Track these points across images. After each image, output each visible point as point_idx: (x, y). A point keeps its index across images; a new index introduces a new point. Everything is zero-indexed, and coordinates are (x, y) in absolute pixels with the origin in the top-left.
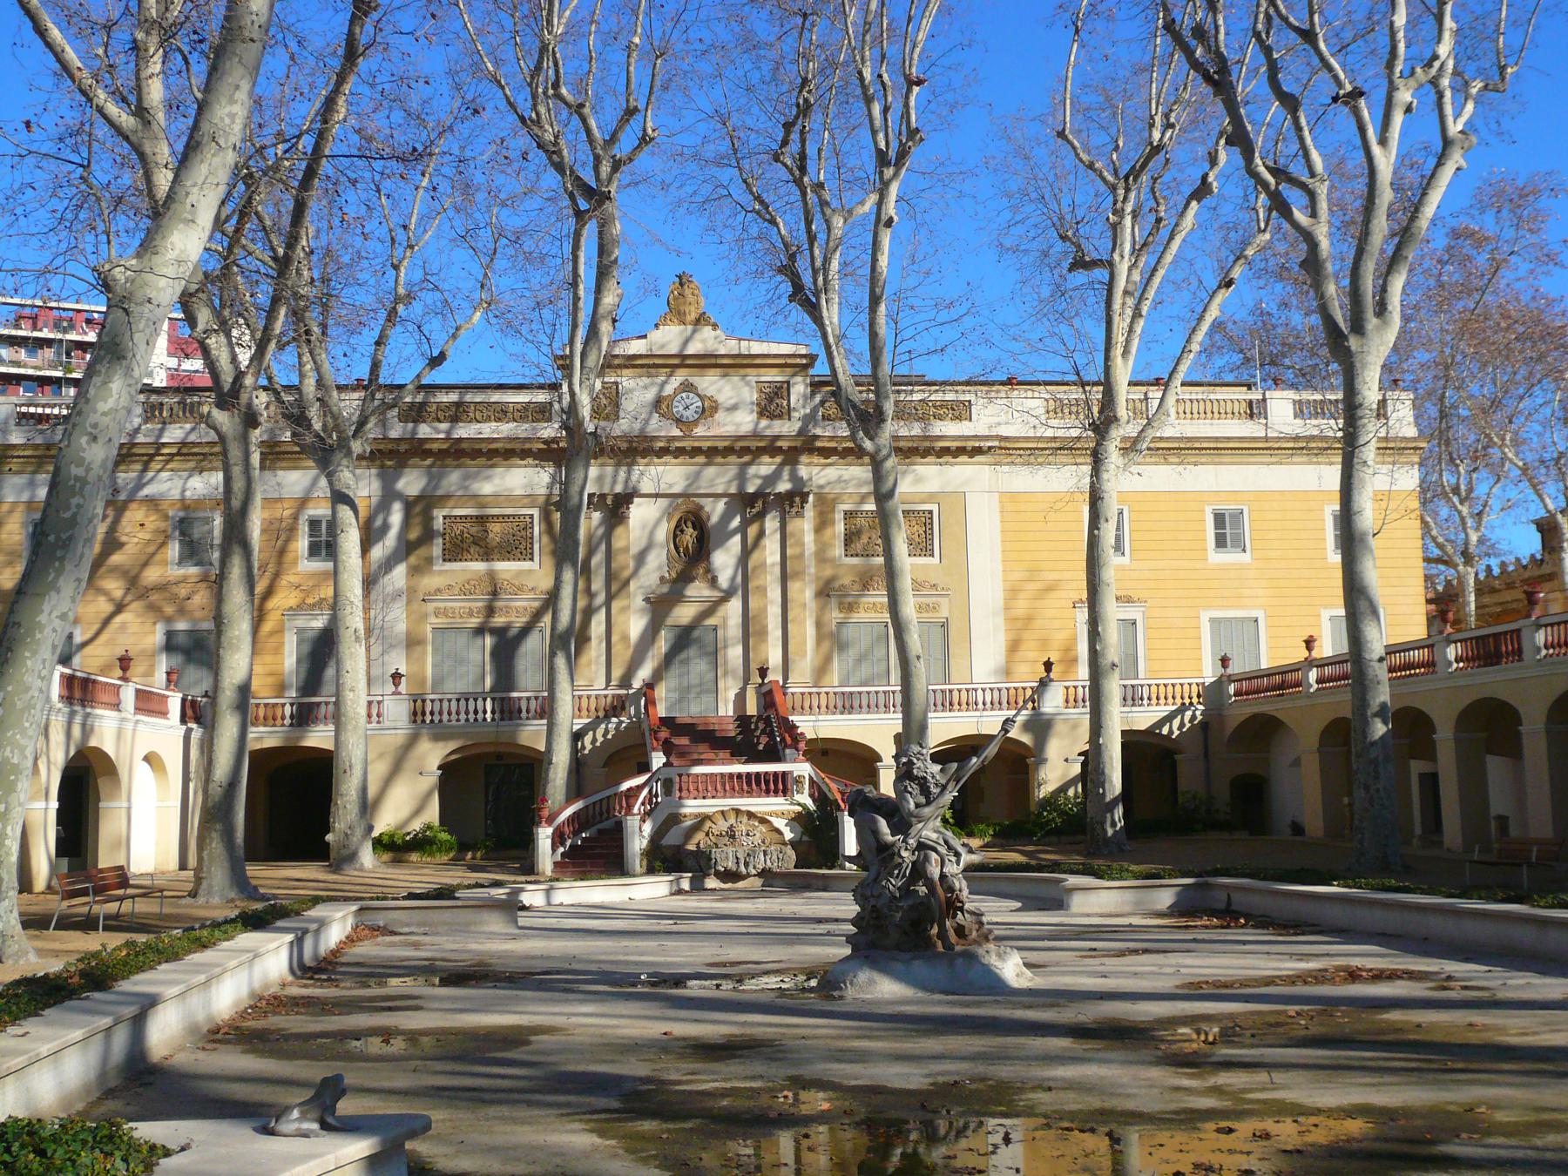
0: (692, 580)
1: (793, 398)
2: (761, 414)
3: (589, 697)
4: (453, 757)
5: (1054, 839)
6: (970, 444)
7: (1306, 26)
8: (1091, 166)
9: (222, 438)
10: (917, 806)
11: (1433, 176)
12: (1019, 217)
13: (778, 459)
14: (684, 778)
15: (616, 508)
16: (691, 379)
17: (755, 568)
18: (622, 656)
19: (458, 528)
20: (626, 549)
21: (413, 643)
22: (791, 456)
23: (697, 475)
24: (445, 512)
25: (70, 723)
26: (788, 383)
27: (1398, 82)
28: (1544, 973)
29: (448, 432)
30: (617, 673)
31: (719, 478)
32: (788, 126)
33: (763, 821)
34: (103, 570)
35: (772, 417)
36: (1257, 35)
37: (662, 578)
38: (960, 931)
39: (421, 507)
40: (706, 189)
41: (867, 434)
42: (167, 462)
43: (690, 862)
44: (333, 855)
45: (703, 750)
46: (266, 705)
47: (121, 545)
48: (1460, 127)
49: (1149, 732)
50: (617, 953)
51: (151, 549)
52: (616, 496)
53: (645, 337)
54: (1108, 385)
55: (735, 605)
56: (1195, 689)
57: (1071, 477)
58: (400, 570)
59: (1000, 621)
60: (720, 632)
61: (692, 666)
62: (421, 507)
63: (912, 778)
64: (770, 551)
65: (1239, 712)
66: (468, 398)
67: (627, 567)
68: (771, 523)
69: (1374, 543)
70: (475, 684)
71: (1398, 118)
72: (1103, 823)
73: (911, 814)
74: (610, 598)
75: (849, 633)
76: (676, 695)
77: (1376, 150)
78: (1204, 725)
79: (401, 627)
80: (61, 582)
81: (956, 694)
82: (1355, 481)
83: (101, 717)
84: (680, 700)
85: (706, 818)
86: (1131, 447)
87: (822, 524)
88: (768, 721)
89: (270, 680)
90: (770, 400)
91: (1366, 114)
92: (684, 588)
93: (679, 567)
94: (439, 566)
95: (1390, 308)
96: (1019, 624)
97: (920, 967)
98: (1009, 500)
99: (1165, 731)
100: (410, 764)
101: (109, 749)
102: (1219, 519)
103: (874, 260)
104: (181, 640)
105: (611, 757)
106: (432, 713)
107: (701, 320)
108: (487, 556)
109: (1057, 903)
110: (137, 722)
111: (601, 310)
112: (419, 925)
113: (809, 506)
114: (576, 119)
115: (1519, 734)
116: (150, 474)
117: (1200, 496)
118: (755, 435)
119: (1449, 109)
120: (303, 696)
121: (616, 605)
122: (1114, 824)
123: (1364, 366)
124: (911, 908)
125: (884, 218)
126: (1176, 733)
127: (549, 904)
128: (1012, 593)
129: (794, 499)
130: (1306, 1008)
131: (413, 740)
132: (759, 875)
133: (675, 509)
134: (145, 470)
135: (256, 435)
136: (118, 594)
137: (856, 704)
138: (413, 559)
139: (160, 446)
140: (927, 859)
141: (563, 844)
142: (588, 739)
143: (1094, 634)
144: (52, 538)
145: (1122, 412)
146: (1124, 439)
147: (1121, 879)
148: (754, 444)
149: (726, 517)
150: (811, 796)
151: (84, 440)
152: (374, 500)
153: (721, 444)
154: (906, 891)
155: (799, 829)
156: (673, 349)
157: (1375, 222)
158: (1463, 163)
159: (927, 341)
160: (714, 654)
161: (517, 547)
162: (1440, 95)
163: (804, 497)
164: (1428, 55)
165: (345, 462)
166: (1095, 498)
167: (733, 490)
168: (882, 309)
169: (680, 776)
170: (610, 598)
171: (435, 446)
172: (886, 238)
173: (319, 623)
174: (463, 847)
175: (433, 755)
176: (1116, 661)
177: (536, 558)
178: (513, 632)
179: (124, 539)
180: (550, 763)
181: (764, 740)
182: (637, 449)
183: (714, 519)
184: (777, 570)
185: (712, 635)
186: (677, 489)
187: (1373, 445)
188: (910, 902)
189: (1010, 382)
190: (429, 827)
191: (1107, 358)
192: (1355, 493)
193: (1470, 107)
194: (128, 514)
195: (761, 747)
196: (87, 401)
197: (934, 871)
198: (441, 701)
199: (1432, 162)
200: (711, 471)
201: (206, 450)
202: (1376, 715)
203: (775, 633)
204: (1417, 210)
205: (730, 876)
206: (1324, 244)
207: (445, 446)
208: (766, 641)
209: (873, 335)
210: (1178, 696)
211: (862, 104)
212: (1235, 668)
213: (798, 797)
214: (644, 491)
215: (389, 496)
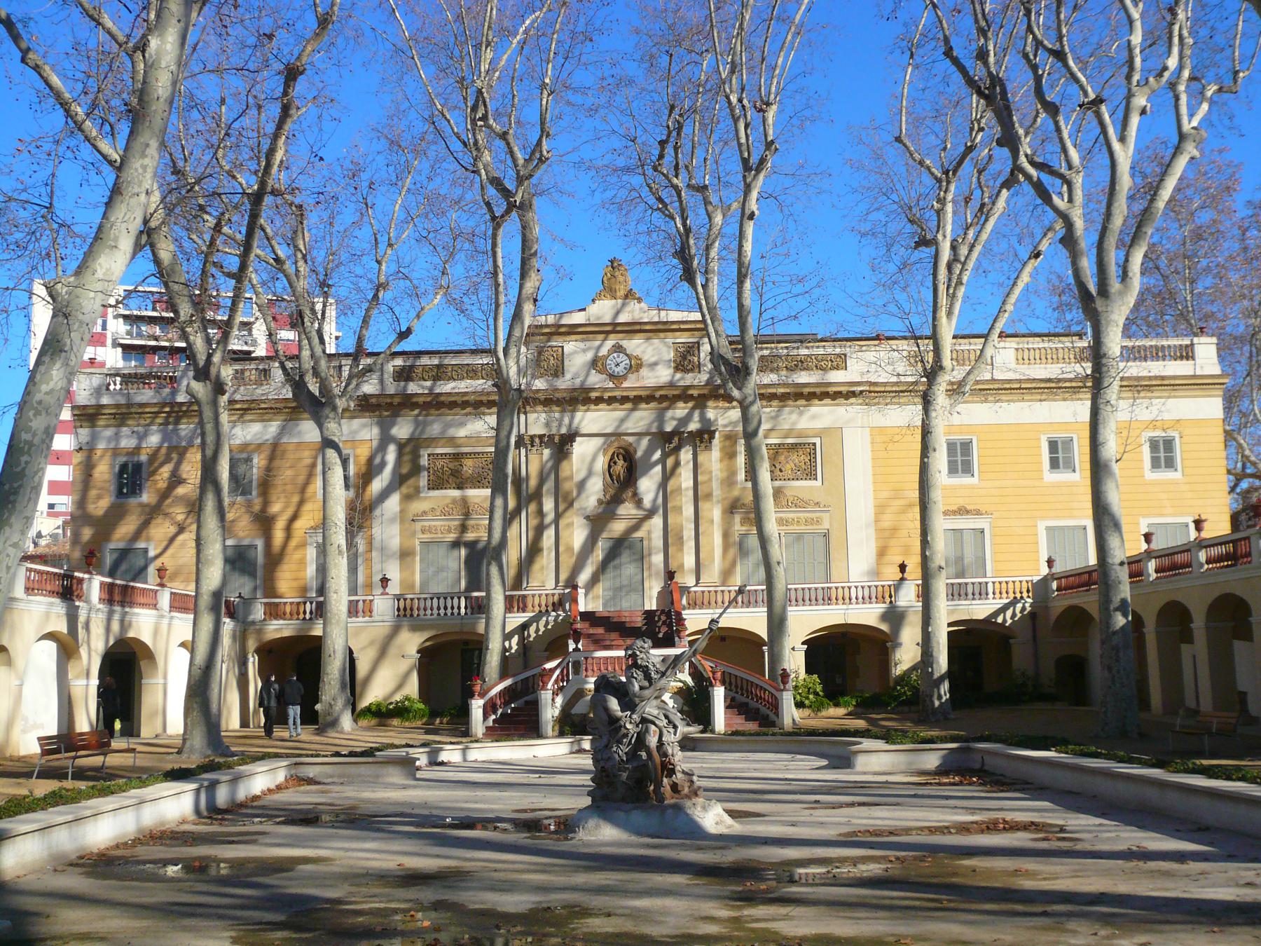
0: (622, 502)
1: (702, 355)
2: (677, 369)
3: (540, 596)
4: (428, 644)
5: (906, 709)
6: (844, 389)
7: (1057, 47)
8: (921, 163)
9: (198, 402)
10: (641, 688)
11: (1169, 165)
12: (876, 206)
13: (690, 405)
14: (590, 661)
15: (562, 445)
16: (621, 343)
17: (672, 492)
18: (567, 563)
19: (440, 463)
20: (571, 478)
21: (405, 555)
22: (700, 402)
24: (430, 451)
25: (109, 620)
26: (698, 343)
27: (1134, 89)
28: (1142, 827)
29: (431, 389)
30: (563, 576)
31: (641, 419)
32: (662, 144)
34: (169, 501)
35: (686, 371)
36: (1026, 56)
37: (600, 502)
38: (675, 787)
39: (410, 448)
40: (623, 194)
41: (734, 385)
44: (321, 720)
46: (291, 603)
48: (1195, 123)
49: (987, 621)
50: (457, 801)
52: (562, 436)
54: (934, 337)
55: (657, 521)
56: (1025, 585)
57: (908, 414)
59: (872, 531)
60: (645, 543)
62: (410, 448)
63: (635, 665)
64: (685, 478)
65: (1060, 604)
66: (446, 362)
68: (686, 455)
69: (1116, 468)
70: (453, 586)
71: (1135, 120)
72: (932, 696)
73: (635, 695)
74: (558, 516)
77: (1116, 146)
78: (1033, 615)
79: (395, 543)
80: (13, 520)
82: (1101, 418)
83: (138, 614)
84: (614, 598)
86: (956, 390)
88: (668, 614)
89: (295, 584)
90: (684, 357)
91: (1106, 117)
92: (616, 508)
93: (612, 491)
95: (1130, 274)
96: (887, 534)
97: (638, 817)
98: (877, 431)
99: (1000, 620)
100: (393, 651)
101: (146, 638)
102: (1053, 445)
103: (741, 246)
105: (550, 644)
106: (418, 609)
107: (629, 295)
108: (460, 487)
109: (843, 761)
110: (172, 618)
112: (340, 776)
113: (716, 441)
114: (502, 144)
115: (1249, 624)
117: (1036, 427)
118: (671, 385)
119: (1184, 110)
121: (562, 523)
122: (940, 697)
123: (1108, 323)
124: (635, 769)
125: (748, 212)
126: (1009, 622)
127: (465, 760)
128: (880, 509)
129: (704, 436)
130: (911, 854)
131: (396, 630)
133: (609, 446)
135: (224, 399)
136: (180, 518)
137: (752, 600)
138: (404, 489)
140: (647, 730)
141: (495, 712)
142: (532, 629)
143: (925, 543)
144: (7, 487)
145: (947, 362)
146: (952, 383)
147: (901, 743)
148: (671, 393)
149: (649, 451)
151: (31, 413)
152: (375, 443)
153: (643, 393)
154: (633, 755)
155: (681, 701)
156: (607, 319)
157: (1116, 205)
158: (1196, 153)
159: (782, 312)
160: (641, 558)
161: (477, 482)
162: (1177, 98)
163: (712, 434)
164: (1160, 68)
165: (332, 415)
166: (926, 432)
167: (654, 430)
168: (748, 285)
169: (586, 658)
170: (558, 516)
171: (421, 400)
172: (750, 228)
174: (434, 714)
175: (411, 643)
176: (943, 564)
179: (184, 476)
180: (487, 649)
181: (664, 629)
182: (580, 398)
183: (639, 454)
184: (691, 493)
185: (639, 544)
186: (609, 431)
187: (1116, 384)
188: (635, 764)
189: (877, 338)
190: (407, 698)
191: (934, 318)
192: (1101, 426)
193: (1205, 106)
194: (188, 455)
195: (661, 635)
196: (35, 384)
197: (653, 741)
199: (1171, 151)
200: (637, 414)
202: (1117, 609)
203: (690, 545)
204: (1155, 194)
206: (1079, 224)
207: (429, 399)
208: (681, 550)
209: (741, 306)
210: (1011, 591)
211: (730, 122)
212: (1058, 568)
213: (680, 676)
214: (584, 431)
215: (385, 439)
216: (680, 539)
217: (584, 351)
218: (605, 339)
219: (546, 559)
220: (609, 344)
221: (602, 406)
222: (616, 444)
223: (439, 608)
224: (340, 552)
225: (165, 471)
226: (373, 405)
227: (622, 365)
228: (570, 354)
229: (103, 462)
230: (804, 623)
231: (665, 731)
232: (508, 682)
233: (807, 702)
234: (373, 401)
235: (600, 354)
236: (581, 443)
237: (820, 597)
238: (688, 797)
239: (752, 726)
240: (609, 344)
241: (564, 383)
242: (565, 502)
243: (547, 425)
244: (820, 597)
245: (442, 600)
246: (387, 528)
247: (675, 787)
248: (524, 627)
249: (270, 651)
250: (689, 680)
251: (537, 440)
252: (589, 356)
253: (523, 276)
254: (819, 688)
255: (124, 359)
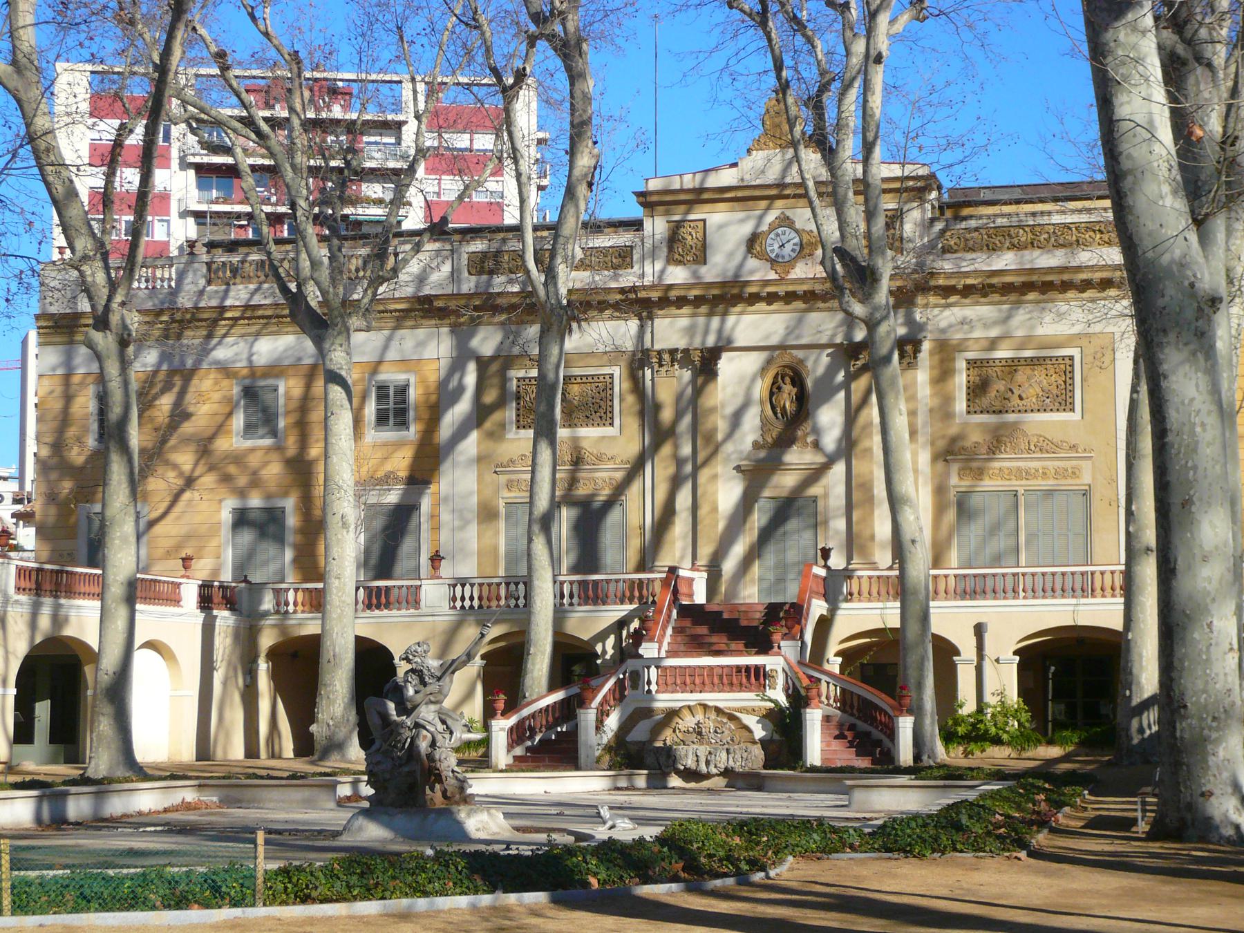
10: (416, 692)
16: (789, 213)
23: (800, 321)
31: (824, 325)
33: (732, 718)
37: (756, 445)
39: (493, 369)
42: (232, 326)
43: (650, 760)
44: (317, 747)
45: (719, 640)
47: (187, 416)
51: (220, 419)
53: (735, 165)
58: (474, 436)
60: (820, 504)
61: (789, 543)
62: (493, 369)
67: (715, 430)
74: (696, 469)
75: (975, 501)
76: (771, 576)
81: (1098, 577)
85: (672, 714)
87: (943, 374)
92: (783, 453)
94: (512, 434)
97: (401, 819)
103: (865, 101)
104: (252, 515)
111: (577, 172)
116: (215, 341)
120: (377, 578)
121: (703, 476)
122: (1141, 730)
125: (873, 53)
132: (721, 774)
134: (210, 336)
138: (488, 425)
139: (222, 309)
149: (831, 371)
150: (786, 690)
155: (771, 726)
167: (838, 340)
172: (878, 76)
173: (392, 498)
177: (617, 422)
178: (596, 505)
179: (191, 409)
180: (529, 654)
182: (729, 295)
186: (774, 340)
194: (195, 382)
197: (423, 745)
198: (481, 585)
200: (814, 317)
201: (269, 313)
205: (691, 775)
214: (739, 343)
216: (870, 500)
217: (742, 221)
218: (768, 208)
219: (680, 526)
220: (771, 216)
221: (762, 306)
222: (780, 362)
223: (463, 599)
224: (345, 525)
225: (166, 402)
226: (440, 309)
227: (789, 247)
228: (721, 227)
229: (85, 392)
230: (1018, 620)
231: (439, 737)
232: (559, 696)
233: (1005, 737)
234: (439, 304)
235: (759, 230)
236: (731, 359)
237: (1039, 587)
238: (458, 803)
239: (863, 763)
240: (771, 216)
241: (712, 271)
242: (708, 447)
243: (690, 331)
244: (1039, 587)
245: (468, 587)
246: (459, 481)
247: (444, 793)
248: (622, 623)
249: (295, 655)
250: (783, 700)
251: (666, 357)
252: (747, 229)
253: (572, 153)
254: (1025, 717)
255: (201, 186)
